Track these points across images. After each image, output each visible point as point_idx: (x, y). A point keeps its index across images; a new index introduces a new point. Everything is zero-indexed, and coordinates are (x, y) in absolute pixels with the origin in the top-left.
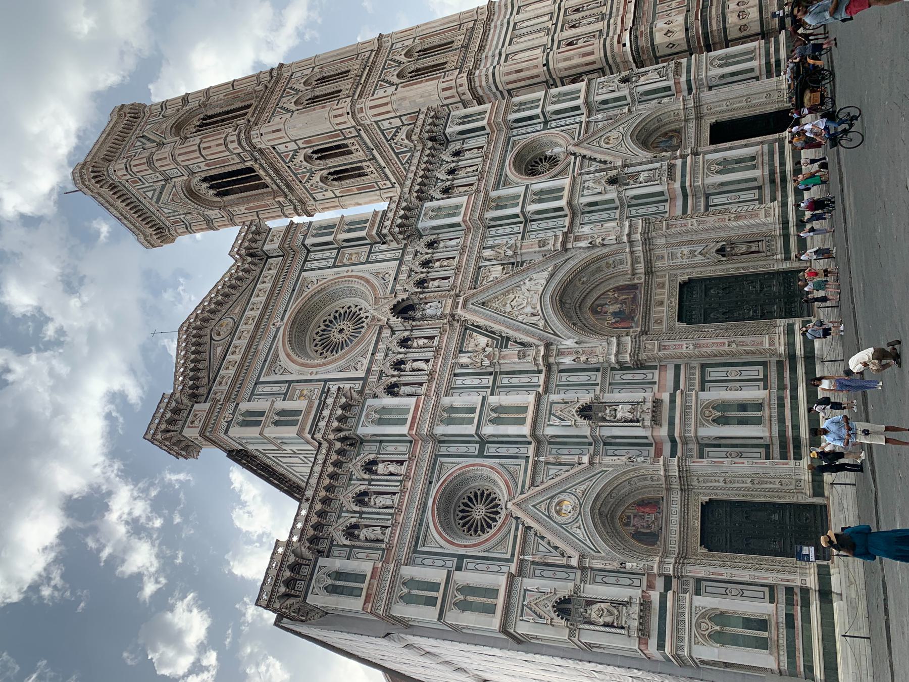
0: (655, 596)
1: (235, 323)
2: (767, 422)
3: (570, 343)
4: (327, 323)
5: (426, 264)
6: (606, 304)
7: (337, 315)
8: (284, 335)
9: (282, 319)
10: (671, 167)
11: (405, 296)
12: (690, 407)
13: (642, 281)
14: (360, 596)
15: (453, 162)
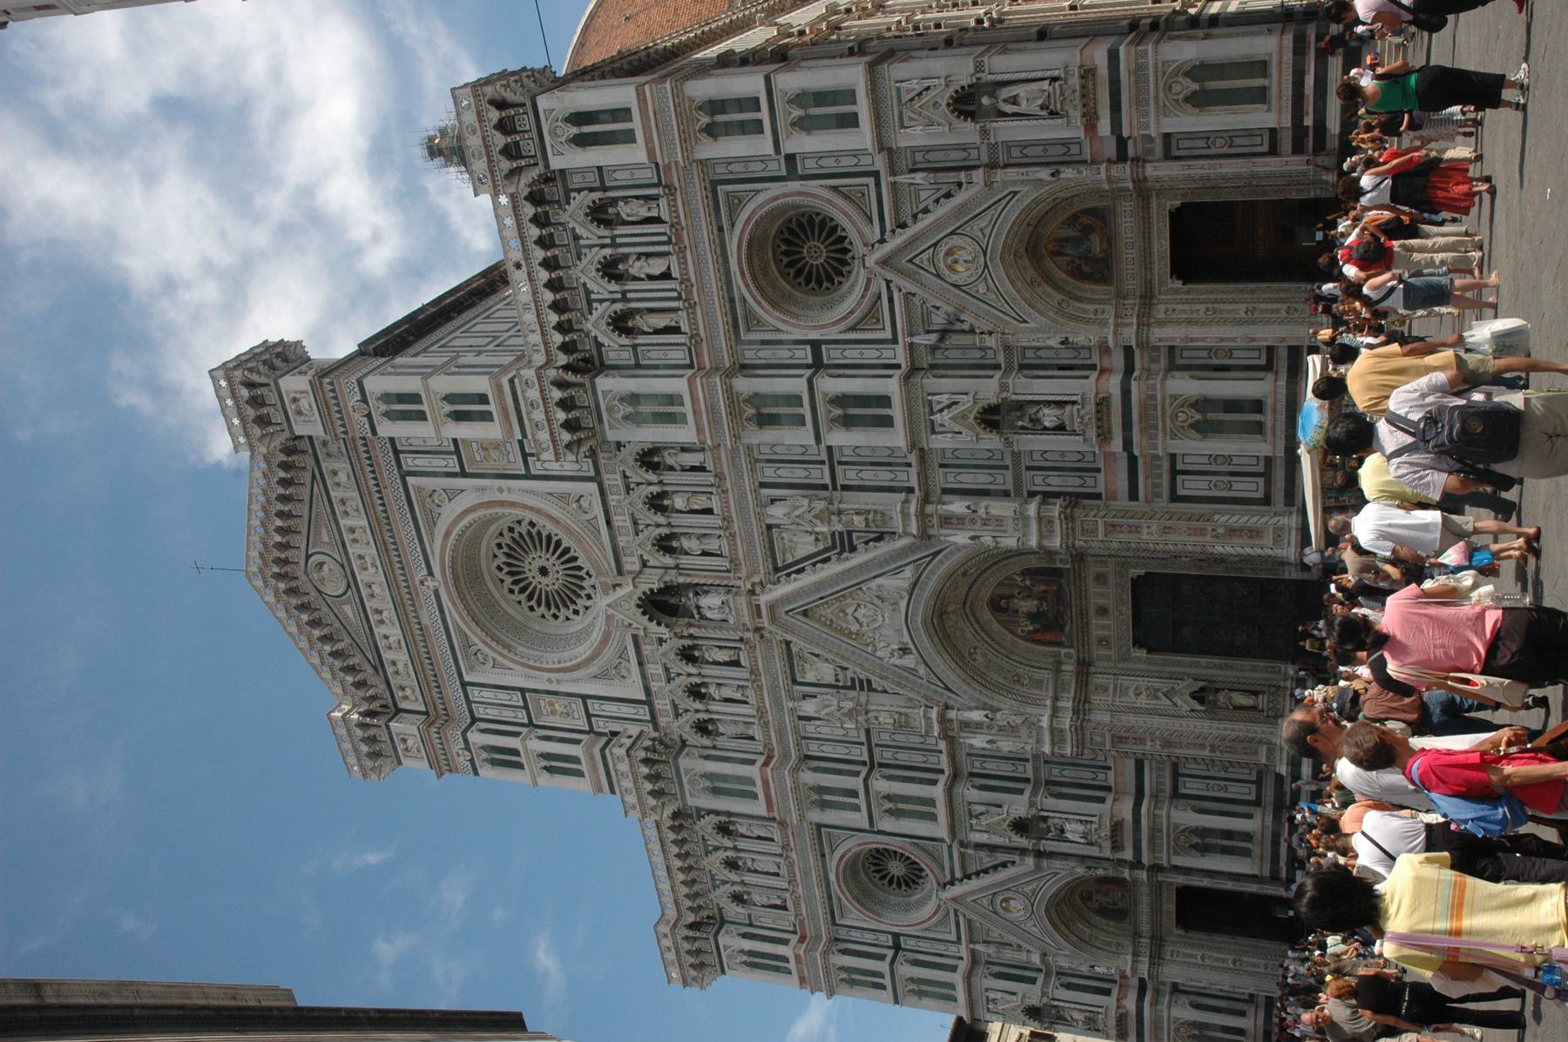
0: (1130, 1004)
1: (342, 566)
2: (1257, 861)
3: (977, 716)
4: (505, 550)
5: (657, 503)
6: (1013, 596)
7: (516, 535)
8: (454, 604)
9: (431, 574)
10: (1103, 404)
11: (655, 587)
12: (1161, 831)
13: (1068, 566)
14: (790, 973)
15: (600, 237)
